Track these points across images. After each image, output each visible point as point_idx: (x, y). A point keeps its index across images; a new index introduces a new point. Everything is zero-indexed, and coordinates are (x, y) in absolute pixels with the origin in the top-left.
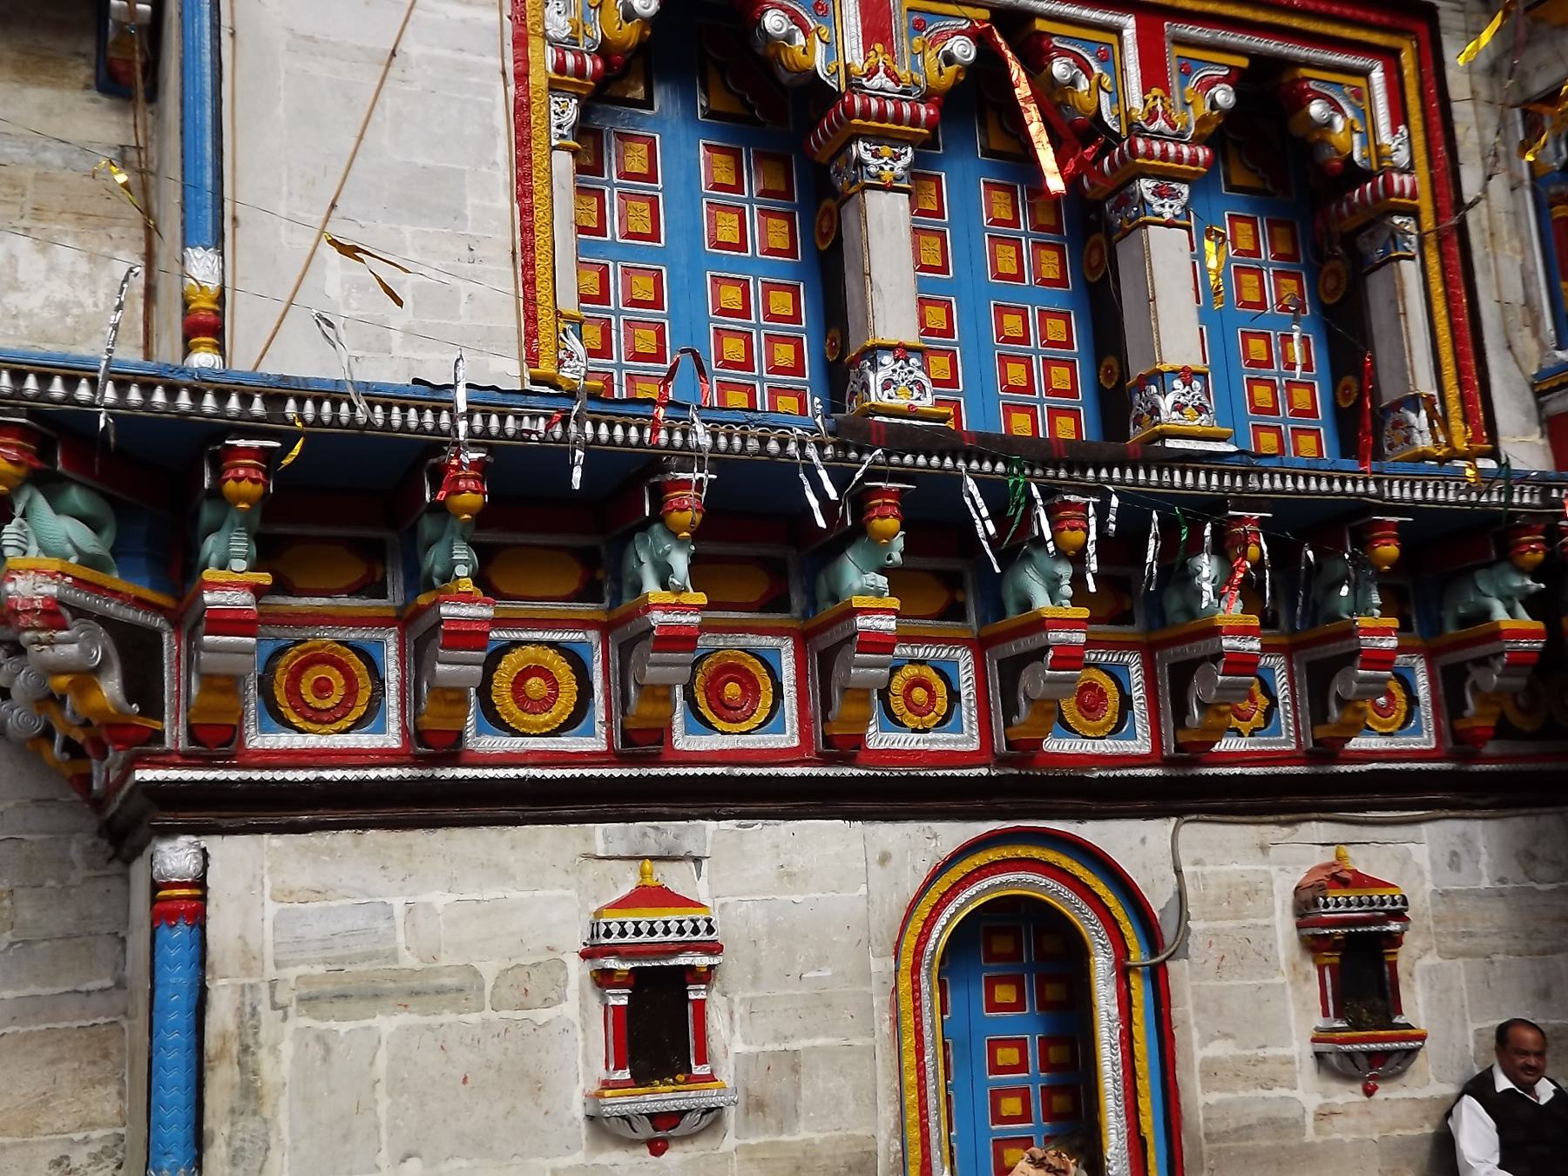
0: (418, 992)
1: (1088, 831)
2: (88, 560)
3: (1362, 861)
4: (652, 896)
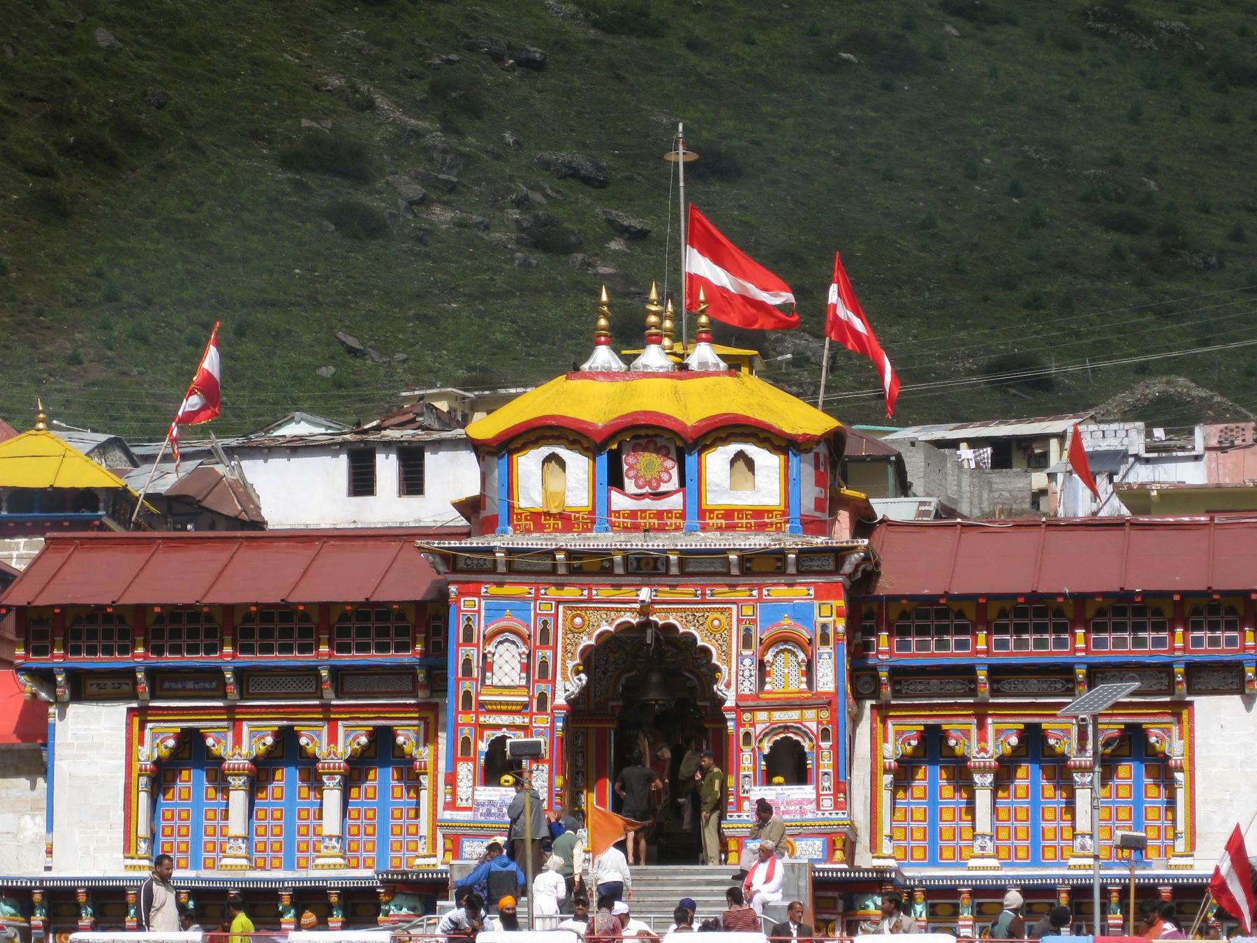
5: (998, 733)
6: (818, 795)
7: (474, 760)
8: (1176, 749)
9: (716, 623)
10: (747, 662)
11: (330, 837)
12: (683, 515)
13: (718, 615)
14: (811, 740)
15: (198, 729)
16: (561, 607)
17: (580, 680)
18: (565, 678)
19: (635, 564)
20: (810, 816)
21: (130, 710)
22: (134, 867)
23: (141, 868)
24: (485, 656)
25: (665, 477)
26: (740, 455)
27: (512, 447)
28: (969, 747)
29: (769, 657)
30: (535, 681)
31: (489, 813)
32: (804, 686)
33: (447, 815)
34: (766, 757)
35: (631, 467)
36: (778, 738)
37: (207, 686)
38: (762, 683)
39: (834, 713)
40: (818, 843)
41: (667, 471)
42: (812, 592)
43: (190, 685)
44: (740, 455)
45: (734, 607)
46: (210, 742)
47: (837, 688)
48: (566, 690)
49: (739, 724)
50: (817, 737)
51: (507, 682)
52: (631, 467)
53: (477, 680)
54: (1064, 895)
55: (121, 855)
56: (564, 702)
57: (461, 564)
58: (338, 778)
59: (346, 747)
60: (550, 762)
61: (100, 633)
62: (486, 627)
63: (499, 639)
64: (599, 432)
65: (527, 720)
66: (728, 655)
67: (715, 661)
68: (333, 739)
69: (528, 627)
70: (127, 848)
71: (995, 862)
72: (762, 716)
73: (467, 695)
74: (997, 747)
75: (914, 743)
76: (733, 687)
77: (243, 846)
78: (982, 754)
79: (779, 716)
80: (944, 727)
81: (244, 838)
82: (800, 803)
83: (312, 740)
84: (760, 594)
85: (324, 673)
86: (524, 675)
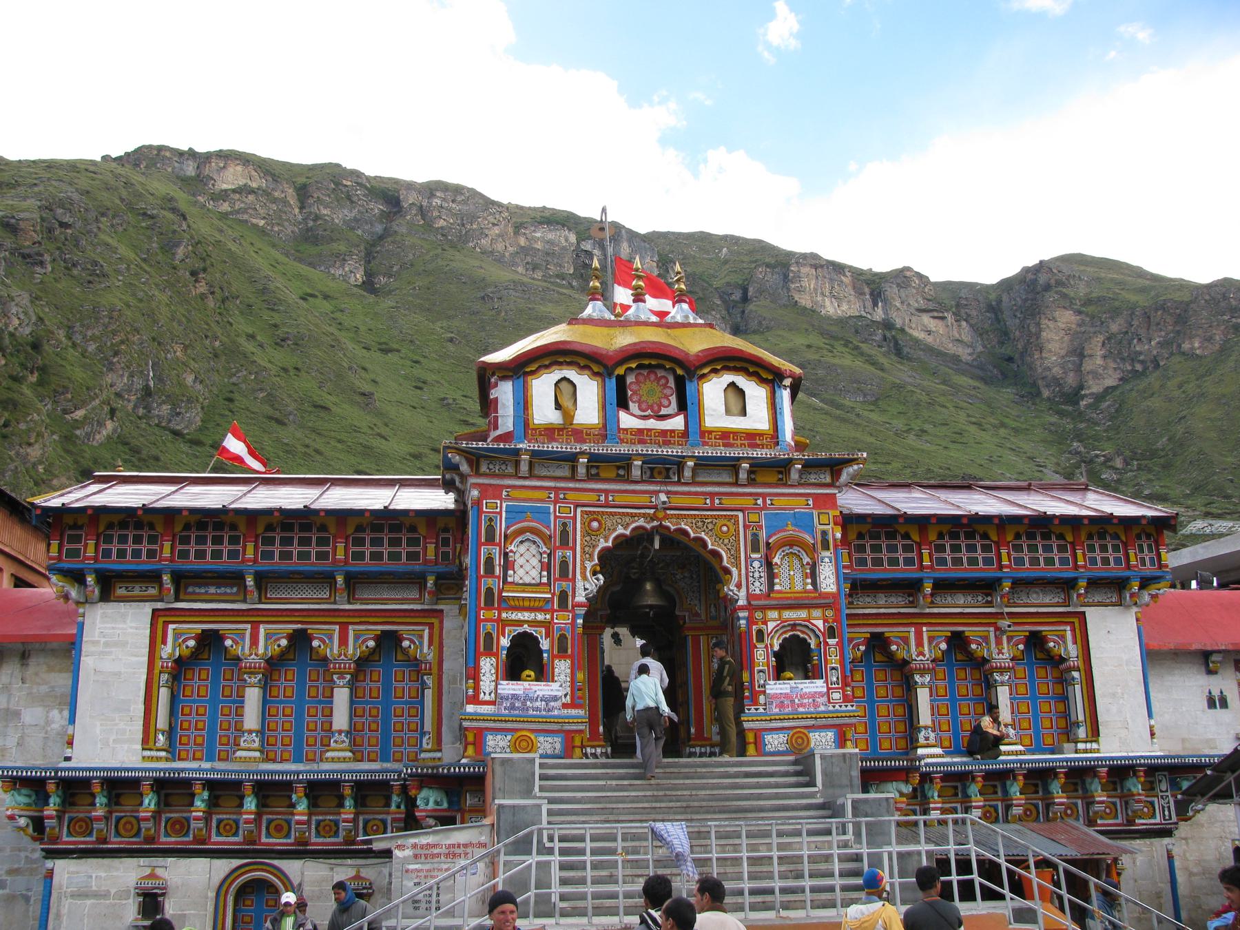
0: (96, 895)
1: (276, 862)
2: (29, 805)
3: (364, 873)
4: (152, 876)
5: (931, 639)
6: (829, 689)
7: (496, 655)
8: (1072, 650)
9: (725, 529)
10: (756, 564)
11: (340, 732)
12: (685, 434)
13: (725, 522)
14: (817, 636)
15: (218, 631)
16: (579, 510)
17: (598, 579)
18: (584, 578)
19: (648, 473)
20: (822, 708)
21: (154, 611)
22: (151, 759)
23: (158, 759)
24: (506, 554)
25: (665, 402)
26: (732, 385)
27: (528, 370)
28: (909, 651)
29: (776, 560)
30: (555, 580)
31: (513, 707)
32: (810, 587)
33: (470, 708)
34: (776, 654)
35: (635, 393)
36: (787, 636)
37: (228, 591)
38: (771, 584)
39: (838, 611)
40: (830, 735)
41: (667, 397)
42: (811, 502)
43: (212, 590)
44: (732, 385)
45: (740, 515)
46: (228, 643)
47: (838, 589)
48: (586, 589)
49: (751, 621)
50: (824, 635)
51: (527, 580)
52: (635, 393)
53: (498, 577)
54: (1021, 778)
55: (140, 747)
56: (584, 600)
57: (484, 469)
58: (348, 677)
59: (355, 648)
60: (572, 657)
61: (130, 539)
62: (508, 527)
63: (520, 539)
64: (610, 358)
65: (548, 616)
66: (737, 558)
67: (725, 563)
68: (343, 641)
69: (548, 527)
70: (145, 741)
71: (938, 751)
72: (773, 614)
73: (489, 591)
74: (930, 651)
75: (862, 648)
76: (744, 589)
77: (257, 740)
78: (921, 657)
79: (788, 614)
80: (887, 635)
81: (257, 732)
82: (813, 696)
83: (324, 642)
84: (764, 502)
85: (340, 579)
86: (545, 573)
